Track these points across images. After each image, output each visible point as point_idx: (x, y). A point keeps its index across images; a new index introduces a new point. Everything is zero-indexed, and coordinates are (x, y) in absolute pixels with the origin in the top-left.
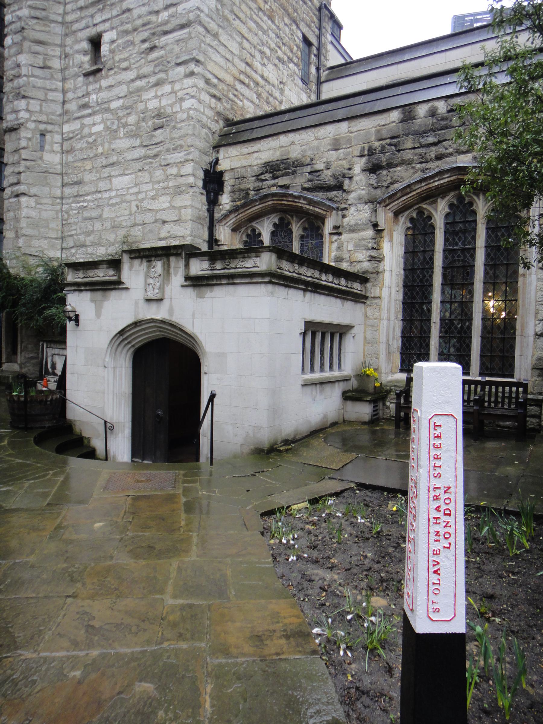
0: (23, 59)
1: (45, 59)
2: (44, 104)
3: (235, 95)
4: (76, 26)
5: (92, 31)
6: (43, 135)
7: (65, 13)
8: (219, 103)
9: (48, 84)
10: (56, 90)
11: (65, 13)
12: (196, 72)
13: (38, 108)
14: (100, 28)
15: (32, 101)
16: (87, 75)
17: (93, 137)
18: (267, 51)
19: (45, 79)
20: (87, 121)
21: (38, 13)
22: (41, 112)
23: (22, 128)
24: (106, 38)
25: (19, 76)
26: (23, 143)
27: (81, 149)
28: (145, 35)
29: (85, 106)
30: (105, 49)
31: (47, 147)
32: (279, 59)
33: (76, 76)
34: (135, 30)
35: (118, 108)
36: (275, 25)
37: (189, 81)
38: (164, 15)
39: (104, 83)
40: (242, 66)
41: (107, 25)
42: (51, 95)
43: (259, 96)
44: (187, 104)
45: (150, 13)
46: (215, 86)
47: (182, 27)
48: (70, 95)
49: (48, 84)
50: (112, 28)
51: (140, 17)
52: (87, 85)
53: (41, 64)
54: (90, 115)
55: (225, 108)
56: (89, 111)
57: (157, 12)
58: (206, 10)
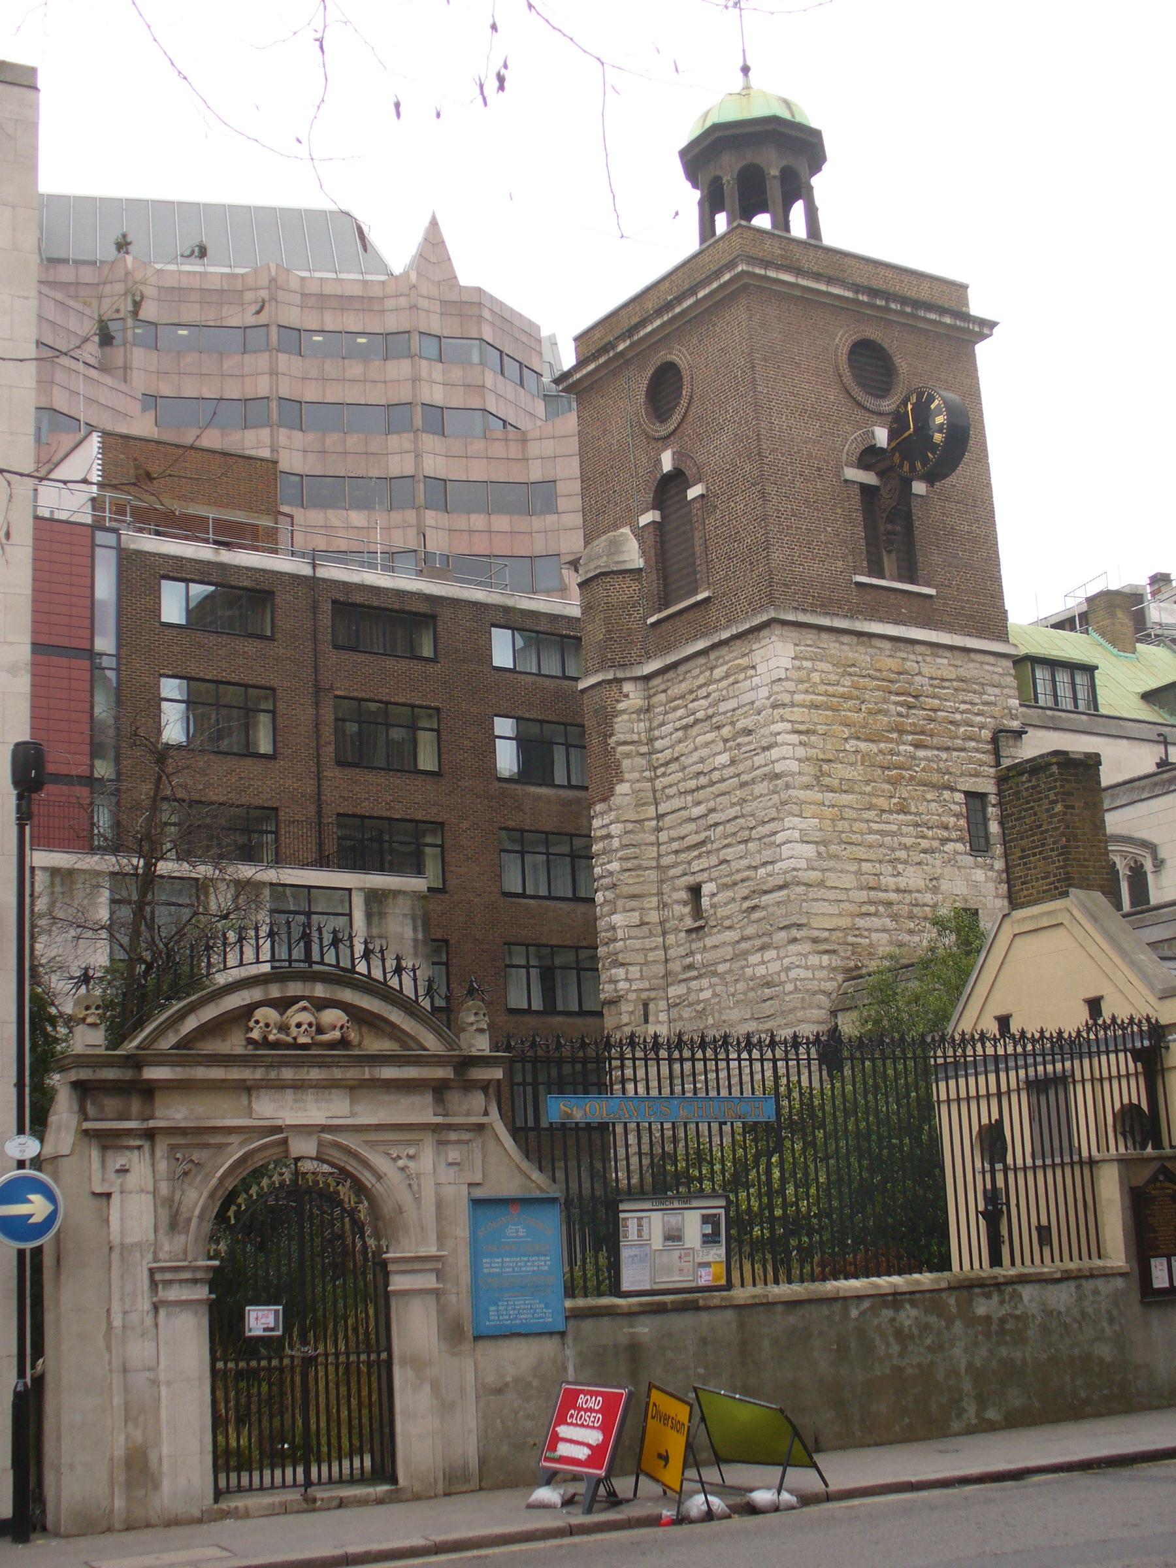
0: (617, 919)
1: (641, 916)
2: (644, 968)
3: (856, 936)
4: (672, 872)
5: (690, 880)
6: (646, 1005)
7: (660, 856)
8: (834, 957)
9: (648, 943)
10: (656, 948)
11: (660, 856)
12: (798, 936)
13: (638, 975)
14: (699, 878)
15: (631, 968)
16: (689, 931)
17: (702, 1005)
18: (902, 854)
19: (643, 938)
20: (694, 984)
21: (629, 865)
22: (642, 978)
23: (623, 1002)
24: (707, 889)
25: (615, 940)
26: (625, 1019)
27: (690, 1019)
28: (746, 892)
29: (690, 967)
30: (705, 901)
31: (651, 1018)
32: (925, 851)
33: (677, 930)
34: (735, 884)
35: (725, 973)
36: (910, 813)
37: (793, 948)
38: (762, 871)
39: (709, 942)
40: (863, 895)
41: (706, 875)
42: (651, 956)
43: (894, 917)
44: (793, 974)
45: (749, 868)
46: (826, 940)
47: (781, 888)
48: (672, 953)
49: (648, 943)
50: (711, 880)
51: (738, 871)
52: (691, 942)
53: (638, 923)
54: (696, 978)
55: (843, 958)
56: (695, 973)
57: (756, 868)
58: (803, 864)
